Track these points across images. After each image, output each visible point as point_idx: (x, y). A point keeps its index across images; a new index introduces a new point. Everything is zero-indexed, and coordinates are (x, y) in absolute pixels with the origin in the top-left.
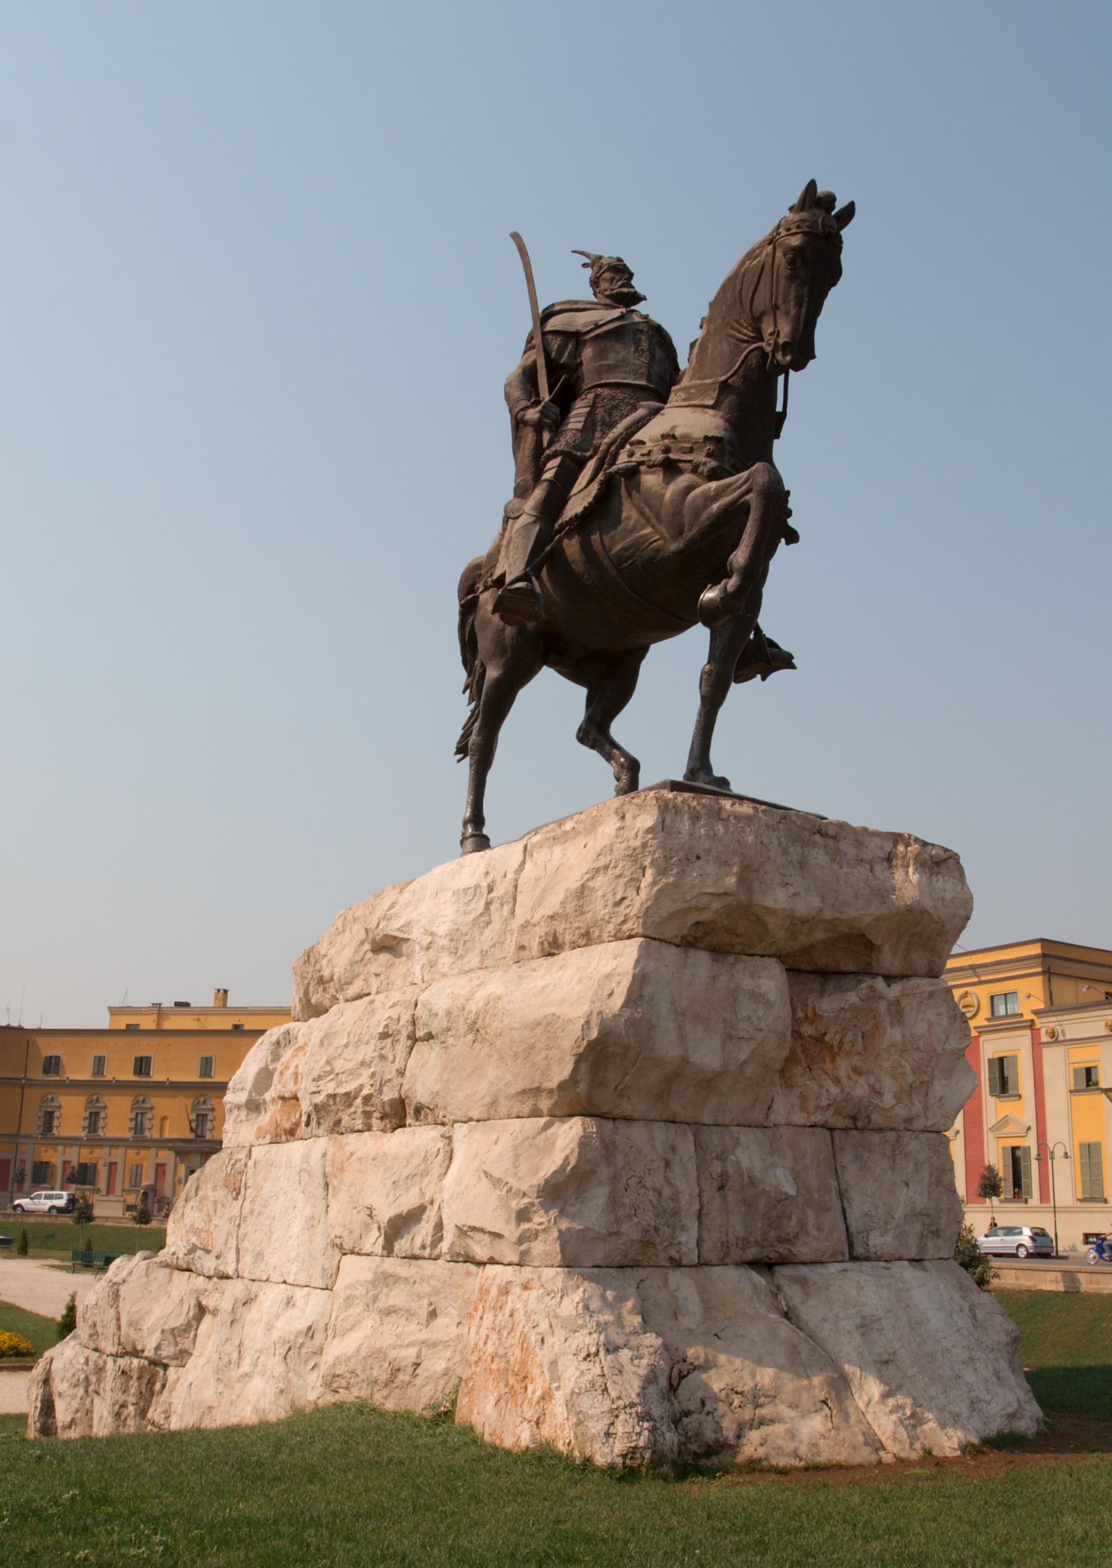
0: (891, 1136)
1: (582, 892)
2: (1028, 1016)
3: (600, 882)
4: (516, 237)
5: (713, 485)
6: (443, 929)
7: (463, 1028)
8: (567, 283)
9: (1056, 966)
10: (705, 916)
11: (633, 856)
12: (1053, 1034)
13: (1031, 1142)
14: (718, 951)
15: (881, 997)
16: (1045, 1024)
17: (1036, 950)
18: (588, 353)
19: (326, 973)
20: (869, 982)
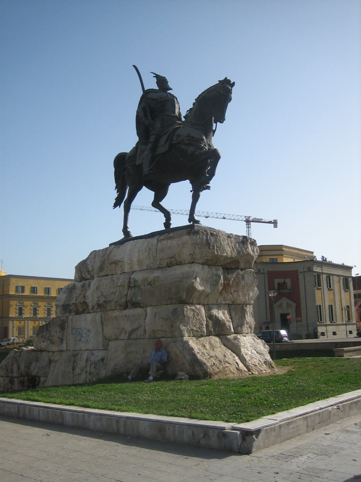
0: (241, 306)
4: (135, 66)
6: (135, 259)
8: (152, 84)
10: (209, 258)
14: (209, 266)
15: (240, 274)
20: (238, 271)
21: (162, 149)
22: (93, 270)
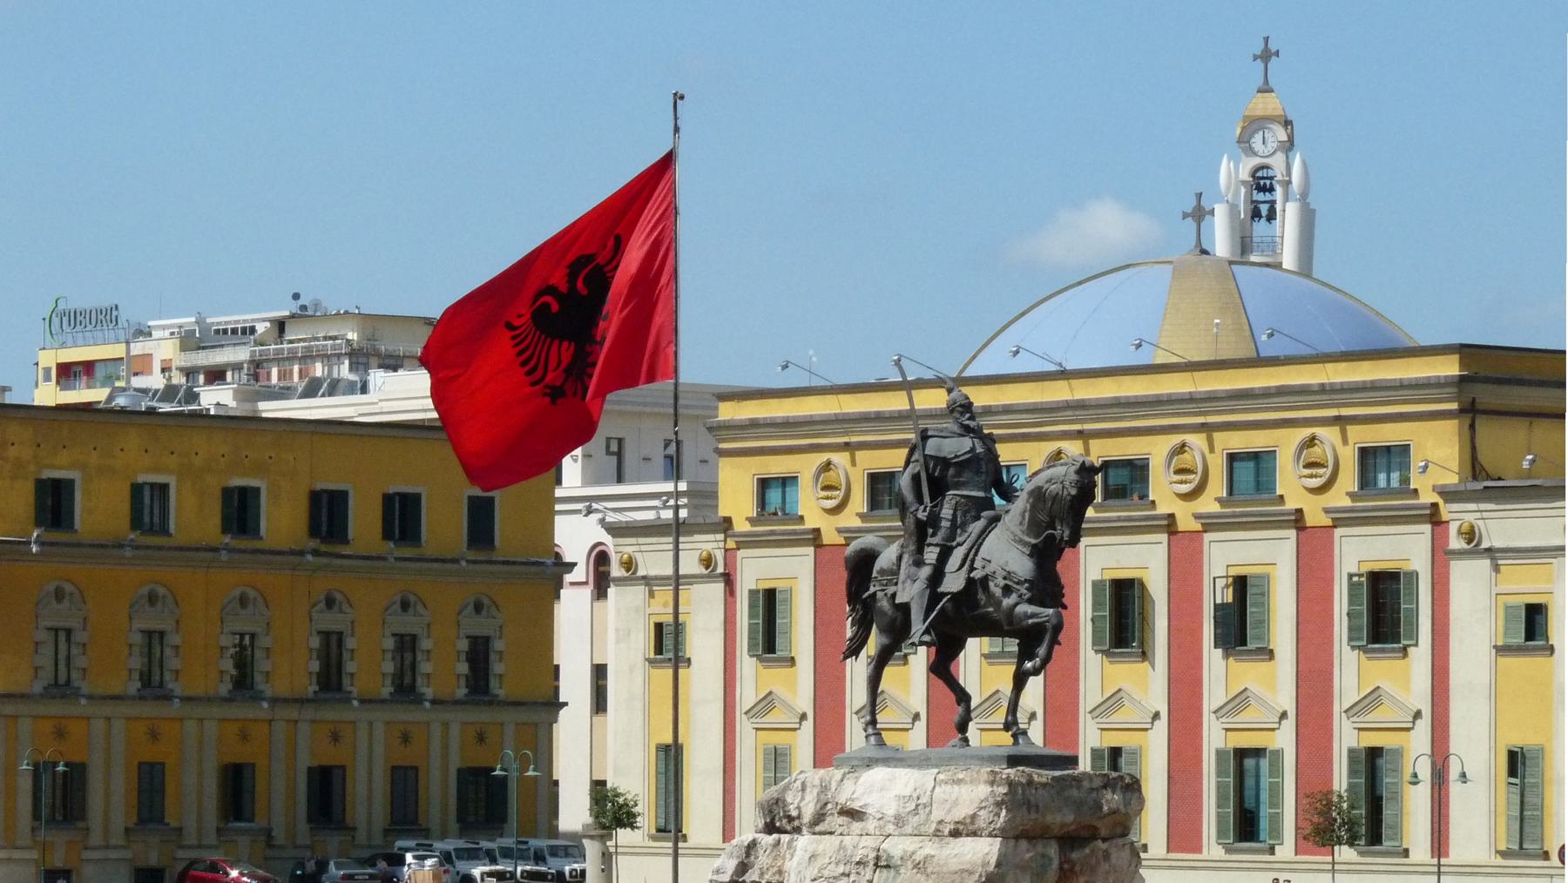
1: (974, 817)
2: (1428, 497)
3: (982, 813)
5: (1031, 609)
6: (890, 812)
7: (910, 865)
9: (1488, 396)
11: (998, 804)
12: (1470, 535)
13: (1418, 743)
16: (1458, 515)
17: (1449, 368)
18: (951, 471)
19: (794, 814)
21: (953, 582)
22: (799, 817)
